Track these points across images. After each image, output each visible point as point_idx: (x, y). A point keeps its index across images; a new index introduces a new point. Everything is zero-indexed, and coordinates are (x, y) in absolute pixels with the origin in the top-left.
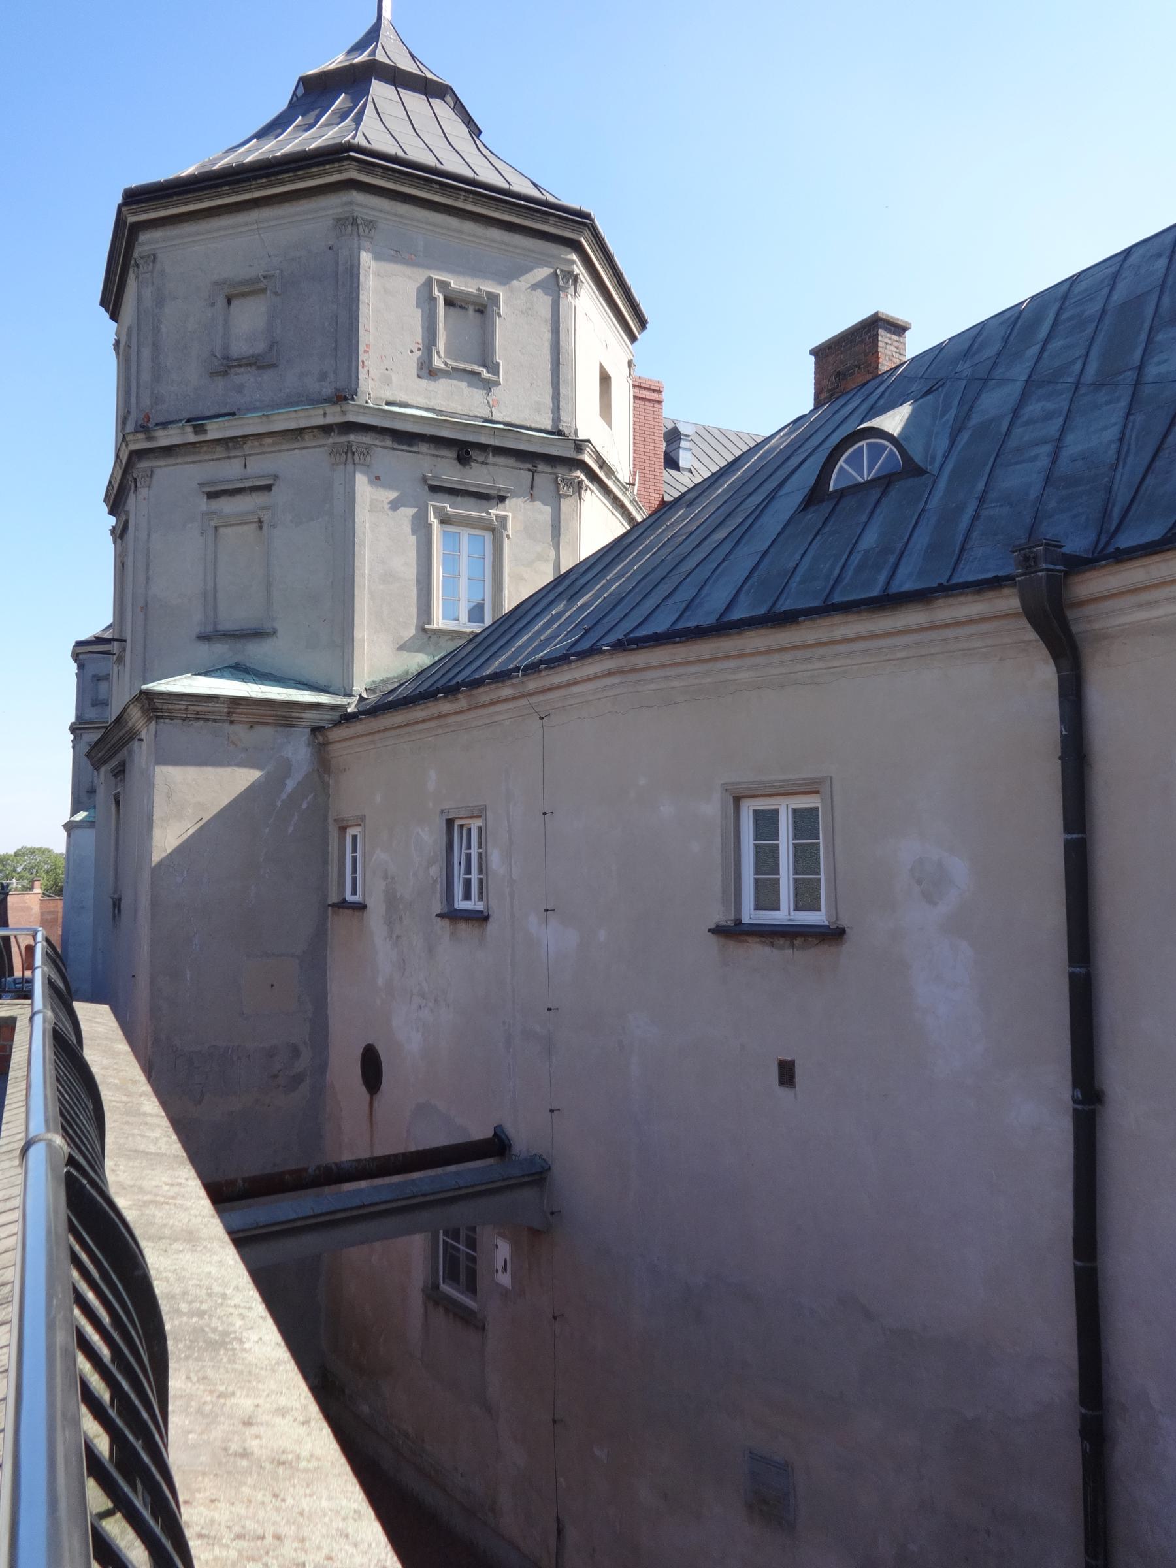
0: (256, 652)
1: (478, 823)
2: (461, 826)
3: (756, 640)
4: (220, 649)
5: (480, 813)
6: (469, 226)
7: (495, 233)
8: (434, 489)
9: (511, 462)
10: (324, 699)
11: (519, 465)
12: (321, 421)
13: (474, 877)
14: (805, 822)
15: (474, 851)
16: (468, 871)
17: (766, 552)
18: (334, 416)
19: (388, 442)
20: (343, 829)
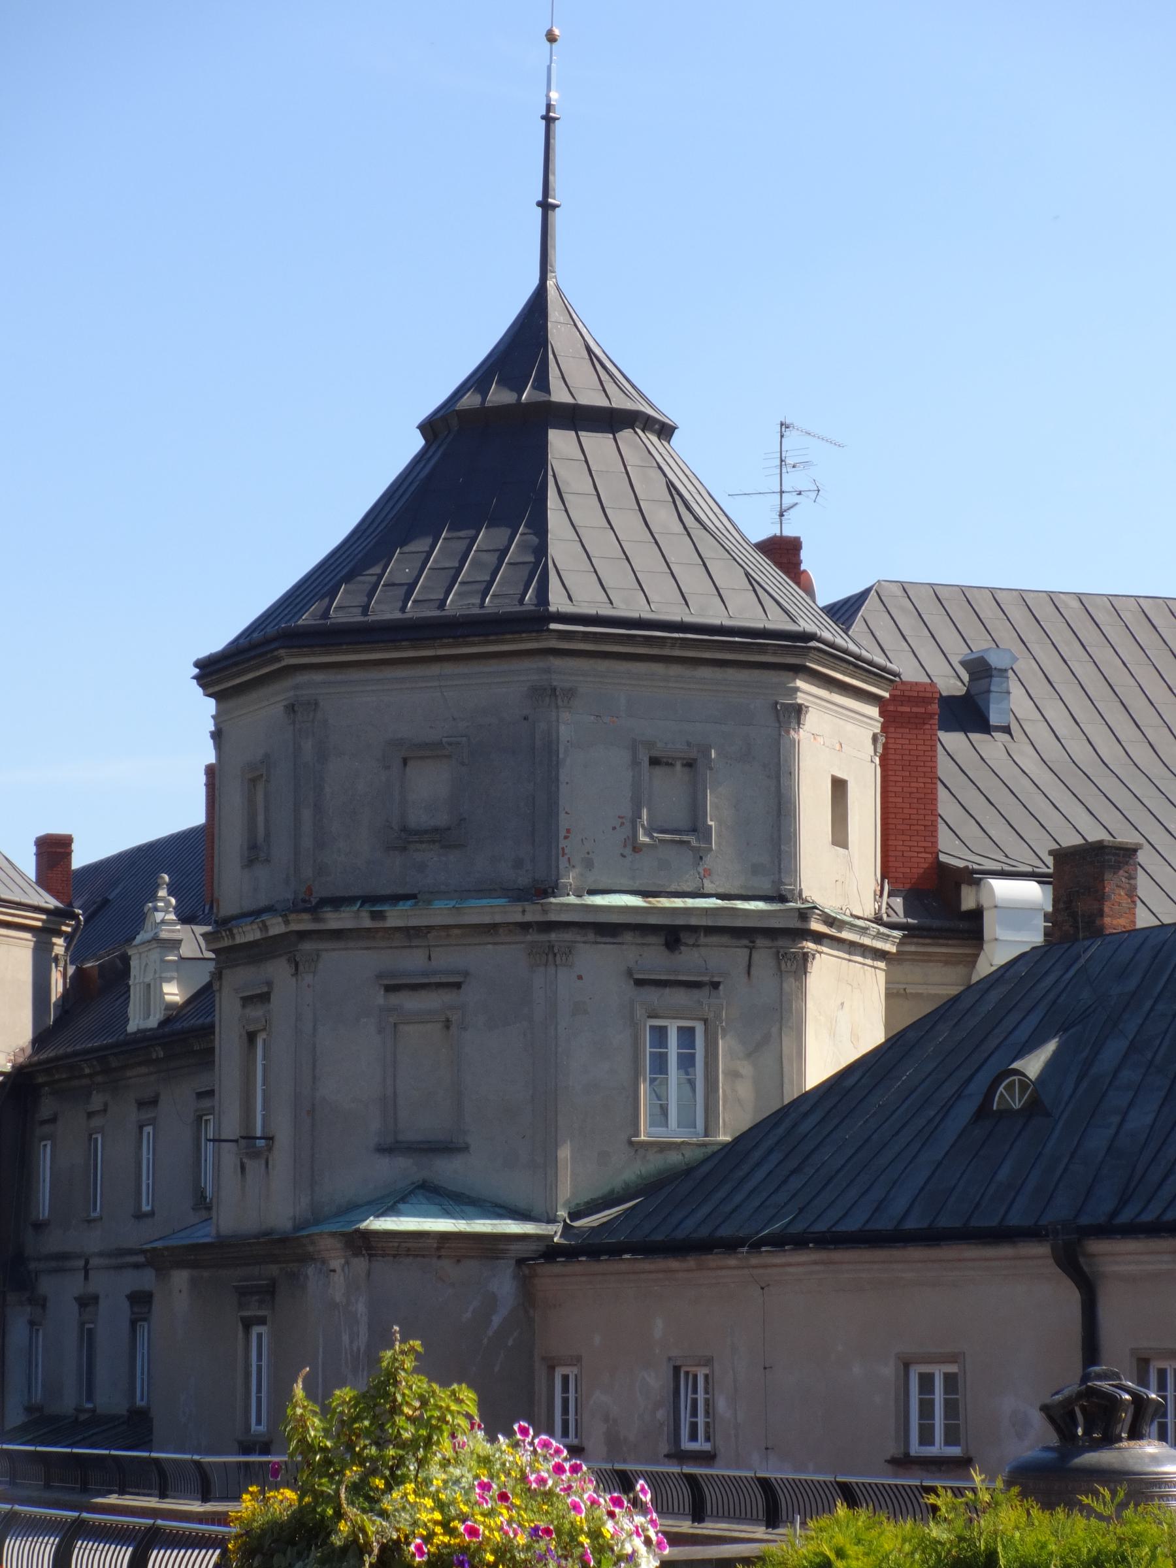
0: (447, 1170)
1: (706, 1370)
2: (687, 1373)
3: (916, 1253)
4: (403, 1163)
5: (708, 1362)
6: (675, 670)
7: (705, 672)
8: (640, 983)
9: (725, 939)
10: (529, 1228)
11: (735, 942)
12: (519, 918)
13: (701, 1420)
14: (951, 1381)
15: (701, 1396)
16: (694, 1413)
17: (940, 1163)
18: (532, 914)
19: (591, 936)
20: (552, 1369)
